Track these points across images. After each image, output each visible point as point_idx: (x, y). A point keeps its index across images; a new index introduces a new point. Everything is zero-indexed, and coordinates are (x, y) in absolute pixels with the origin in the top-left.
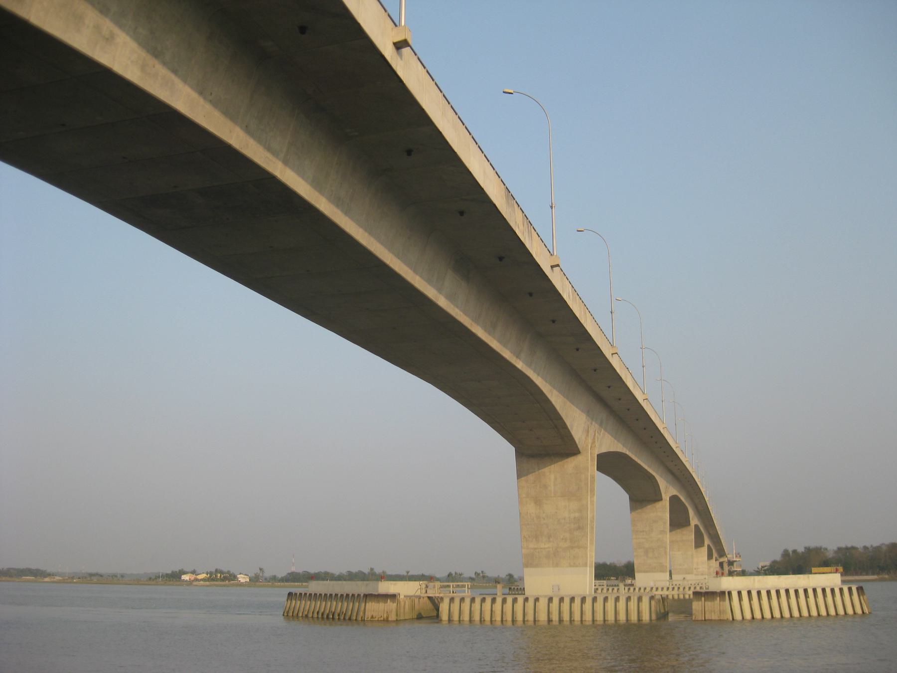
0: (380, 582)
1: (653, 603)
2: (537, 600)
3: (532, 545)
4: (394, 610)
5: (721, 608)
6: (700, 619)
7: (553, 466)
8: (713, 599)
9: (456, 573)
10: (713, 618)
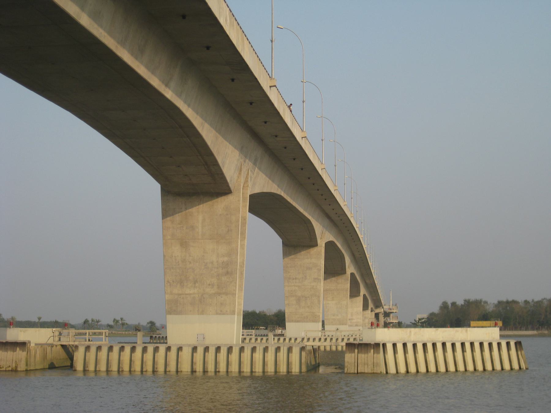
0: (8, 329)
1: (303, 354)
2: (180, 349)
3: (176, 291)
5: (375, 361)
6: (352, 371)
7: (201, 205)
8: (367, 352)
9: (92, 320)
10: (366, 371)
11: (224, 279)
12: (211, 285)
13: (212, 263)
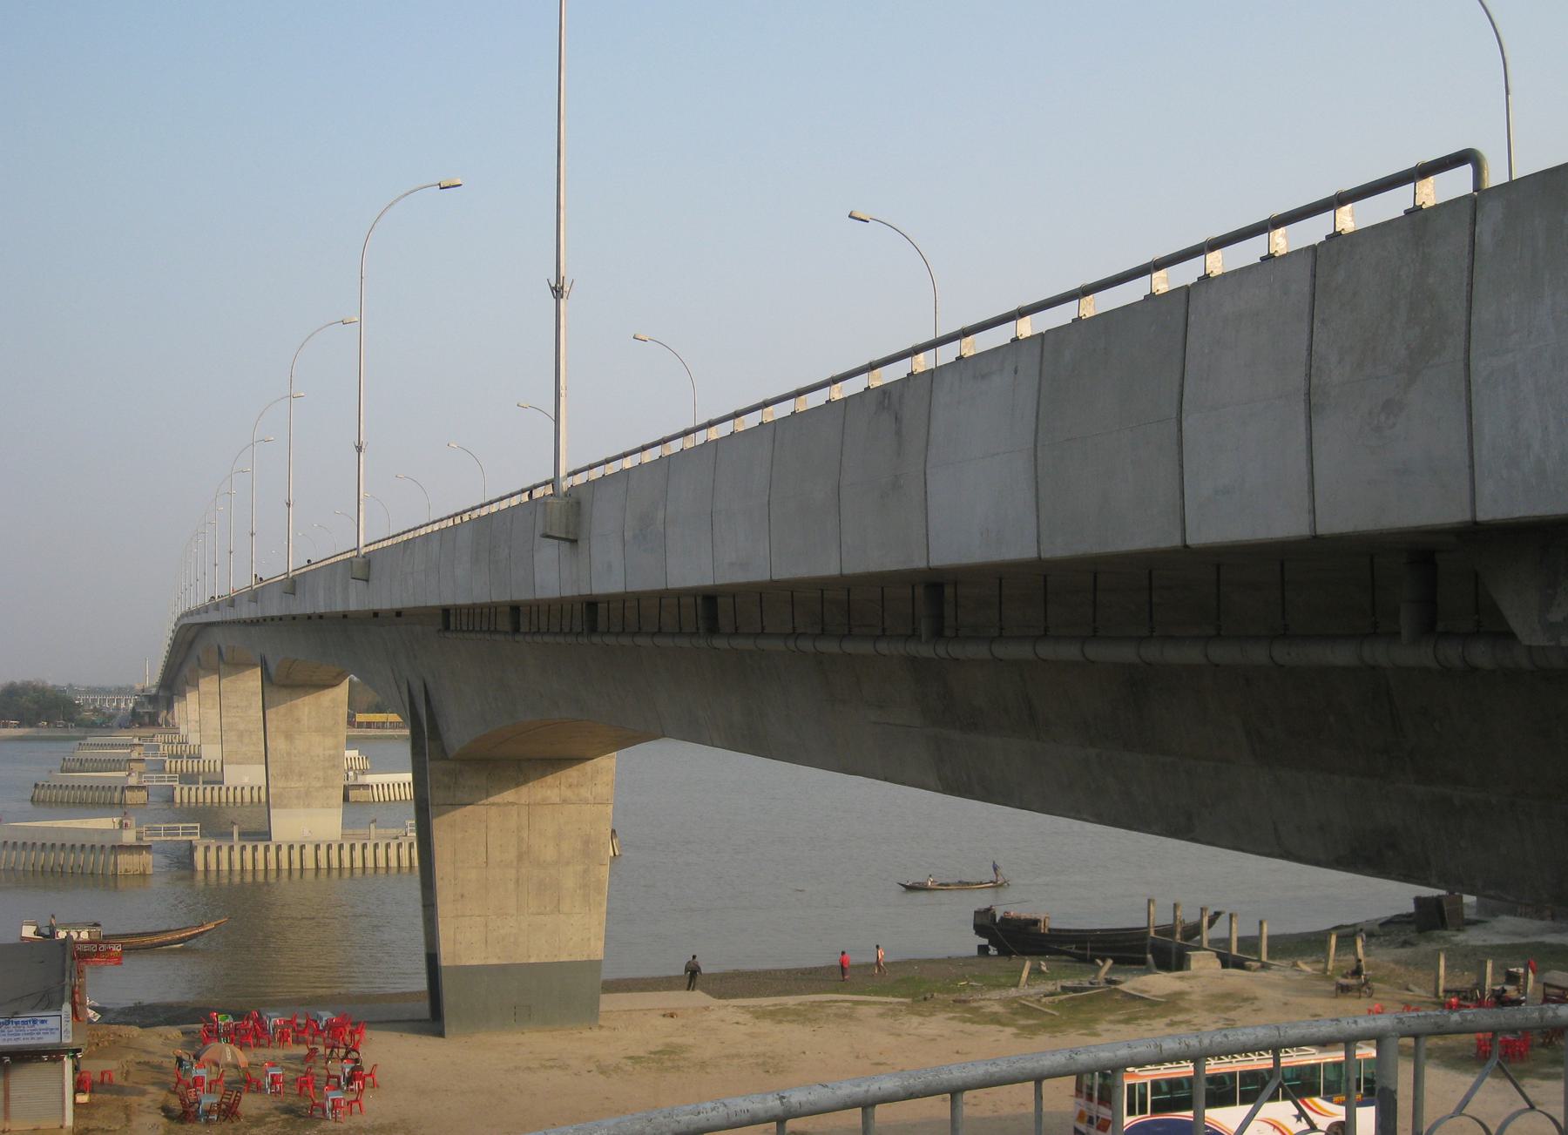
2: (302, 847)
3: (280, 784)
4: (151, 862)
7: (307, 697)
11: (330, 772)
12: (317, 778)
13: (318, 756)
